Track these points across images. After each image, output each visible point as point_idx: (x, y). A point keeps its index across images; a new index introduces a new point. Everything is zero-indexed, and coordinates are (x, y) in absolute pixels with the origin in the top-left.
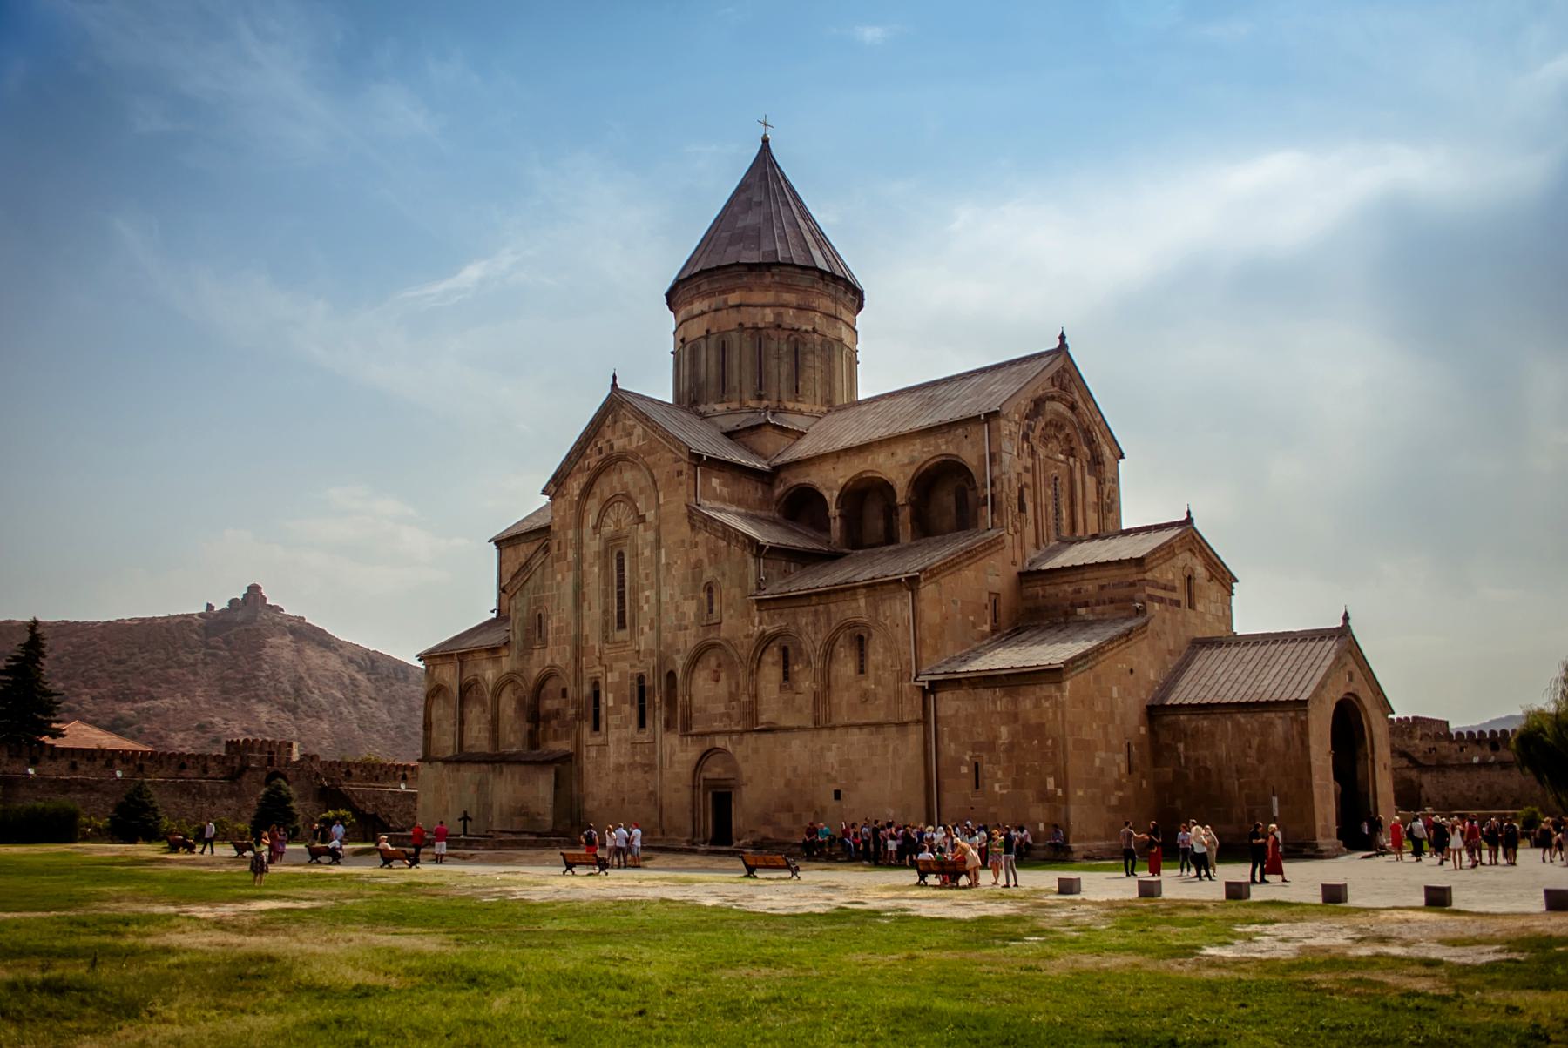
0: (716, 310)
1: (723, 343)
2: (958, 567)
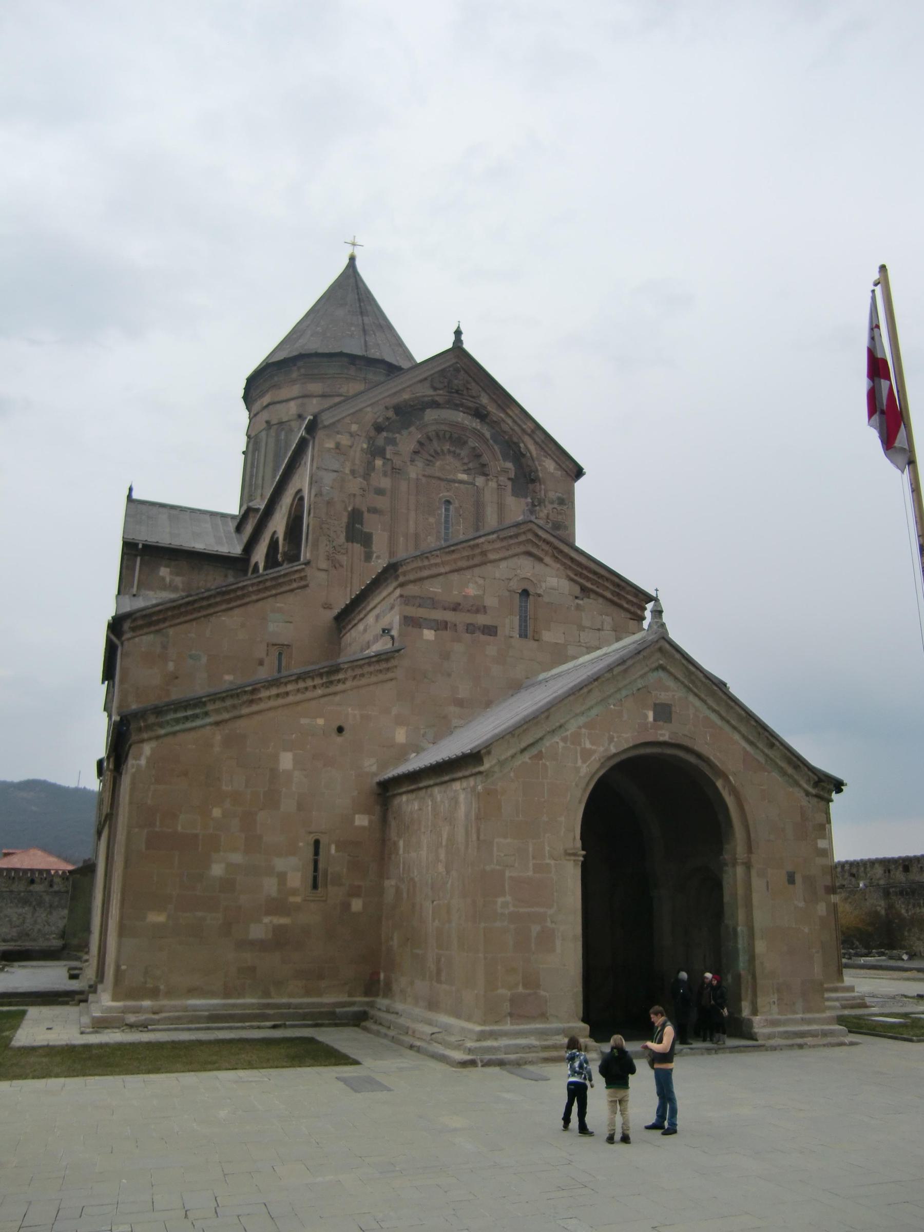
0: (255, 415)
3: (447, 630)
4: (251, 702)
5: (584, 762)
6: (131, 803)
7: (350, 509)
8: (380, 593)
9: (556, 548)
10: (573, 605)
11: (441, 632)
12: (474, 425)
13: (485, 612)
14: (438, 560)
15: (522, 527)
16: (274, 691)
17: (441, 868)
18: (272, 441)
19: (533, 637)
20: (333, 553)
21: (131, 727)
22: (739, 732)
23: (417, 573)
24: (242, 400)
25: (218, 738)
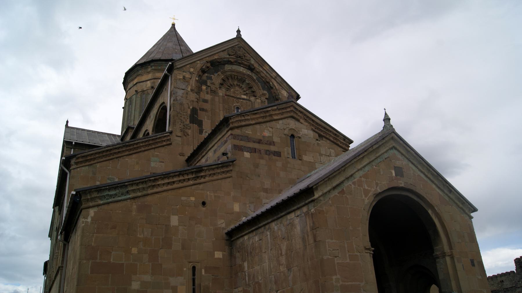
1: (131, 101)
2: (116, 156)
3: (256, 153)
4: (154, 186)
5: (366, 197)
6: (81, 245)
7: (191, 108)
8: (216, 138)
9: (305, 115)
10: (316, 143)
11: (253, 154)
12: (248, 73)
13: (274, 145)
14: (249, 118)
15: (288, 104)
16: (166, 181)
17: (282, 269)
18: (139, 99)
19: (299, 158)
20: (184, 128)
21: (82, 199)
22: (435, 184)
23: (238, 123)
24: (122, 84)
25: (135, 207)
